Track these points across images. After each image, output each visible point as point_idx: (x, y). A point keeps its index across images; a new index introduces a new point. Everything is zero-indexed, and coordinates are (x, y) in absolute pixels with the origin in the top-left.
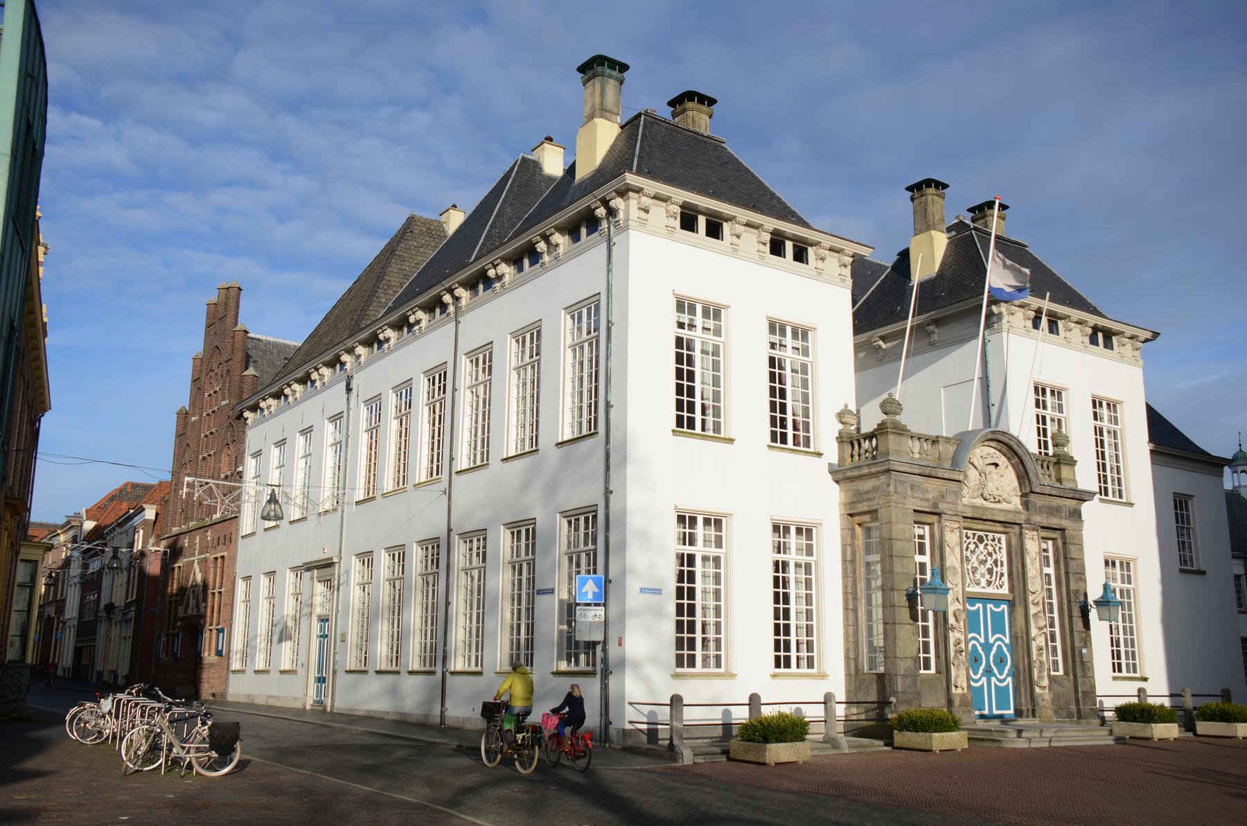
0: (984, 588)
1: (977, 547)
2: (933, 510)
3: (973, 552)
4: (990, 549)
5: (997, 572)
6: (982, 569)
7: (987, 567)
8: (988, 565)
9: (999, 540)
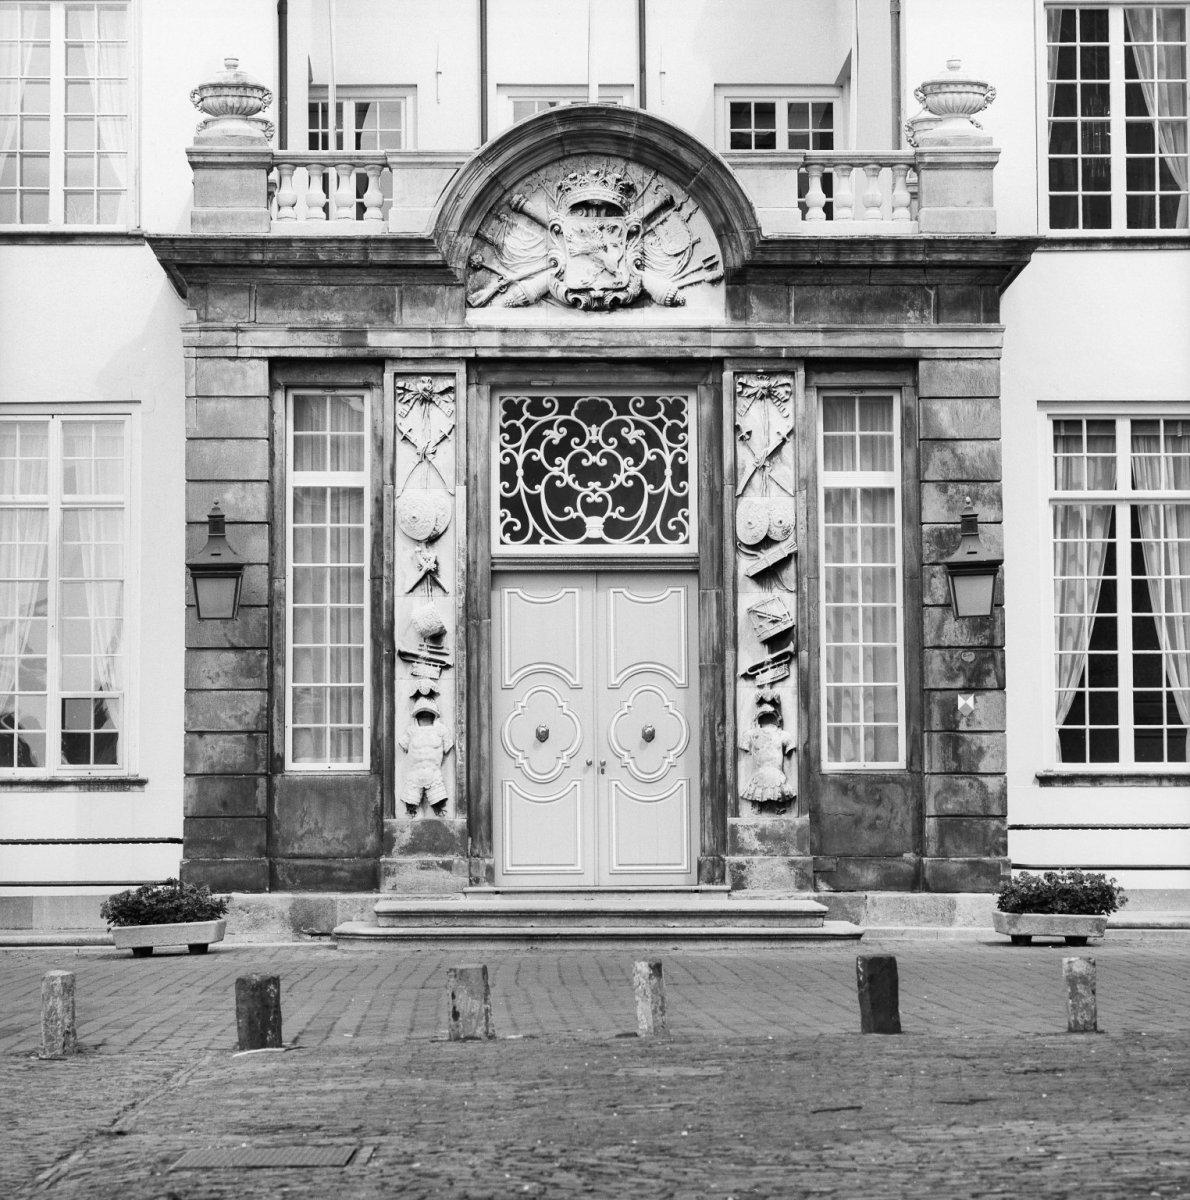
0: (600, 541)
1: (575, 430)
4: (633, 436)
5: (655, 500)
6: (594, 492)
7: (612, 486)
8: (620, 478)
9: (676, 410)
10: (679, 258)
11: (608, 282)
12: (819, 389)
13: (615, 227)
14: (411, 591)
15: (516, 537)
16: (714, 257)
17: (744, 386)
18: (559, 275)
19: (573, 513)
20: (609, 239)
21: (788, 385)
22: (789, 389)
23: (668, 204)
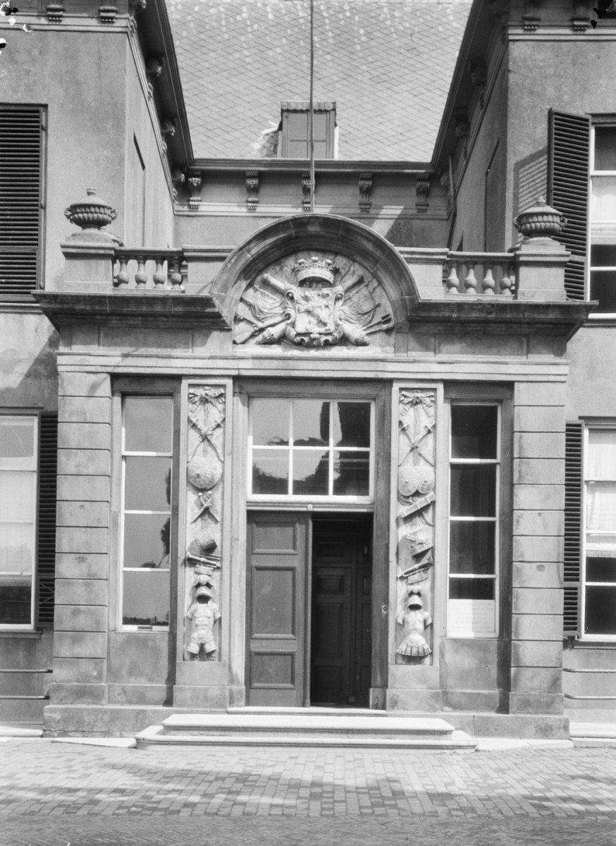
10: (366, 316)
11: (322, 330)
12: (452, 400)
13: (328, 295)
14: (195, 521)
16: (388, 315)
17: (405, 396)
18: (293, 325)
20: (323, 302)
21: (432, 396)
22: (433, 399)
23: (360, 281)
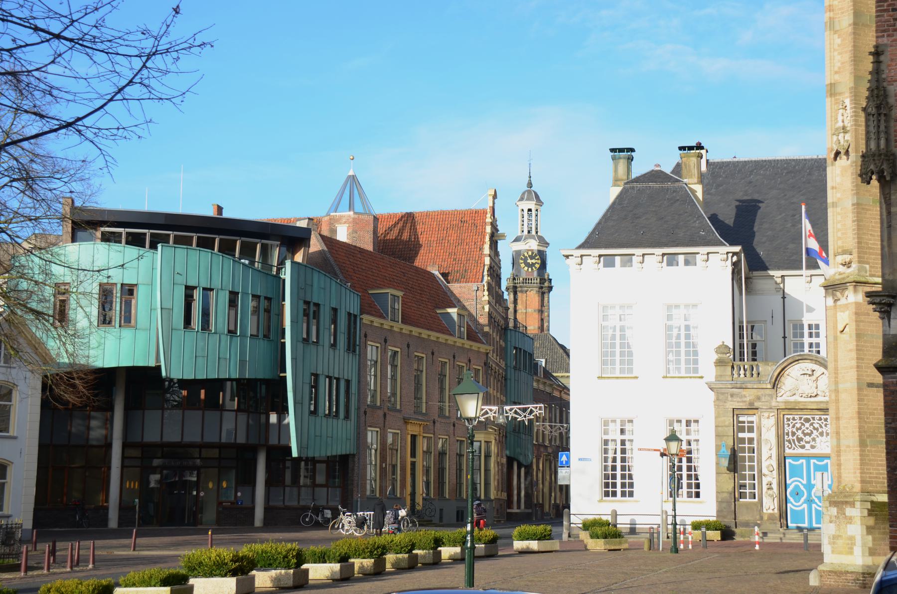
2: (749, 407)
3: (798, 429)
4: (816, 426)
6: (807, 438)
8: (813, 436)
15: (790, 448)
19: (802, 443)
23: (823, 373)
